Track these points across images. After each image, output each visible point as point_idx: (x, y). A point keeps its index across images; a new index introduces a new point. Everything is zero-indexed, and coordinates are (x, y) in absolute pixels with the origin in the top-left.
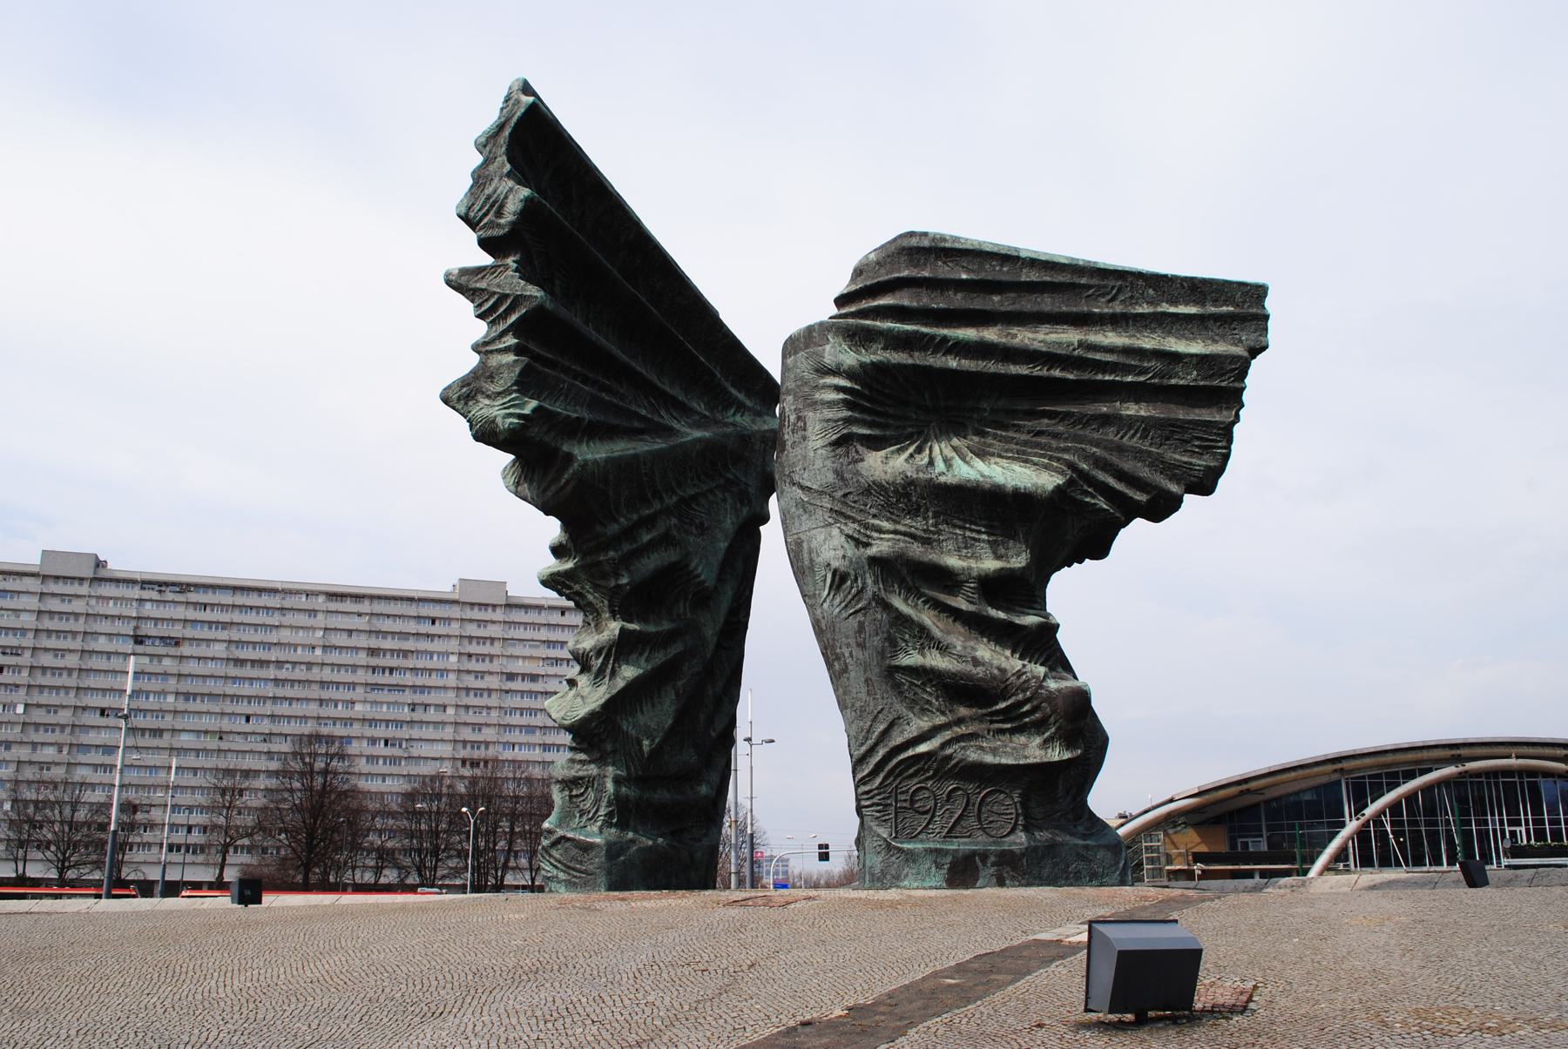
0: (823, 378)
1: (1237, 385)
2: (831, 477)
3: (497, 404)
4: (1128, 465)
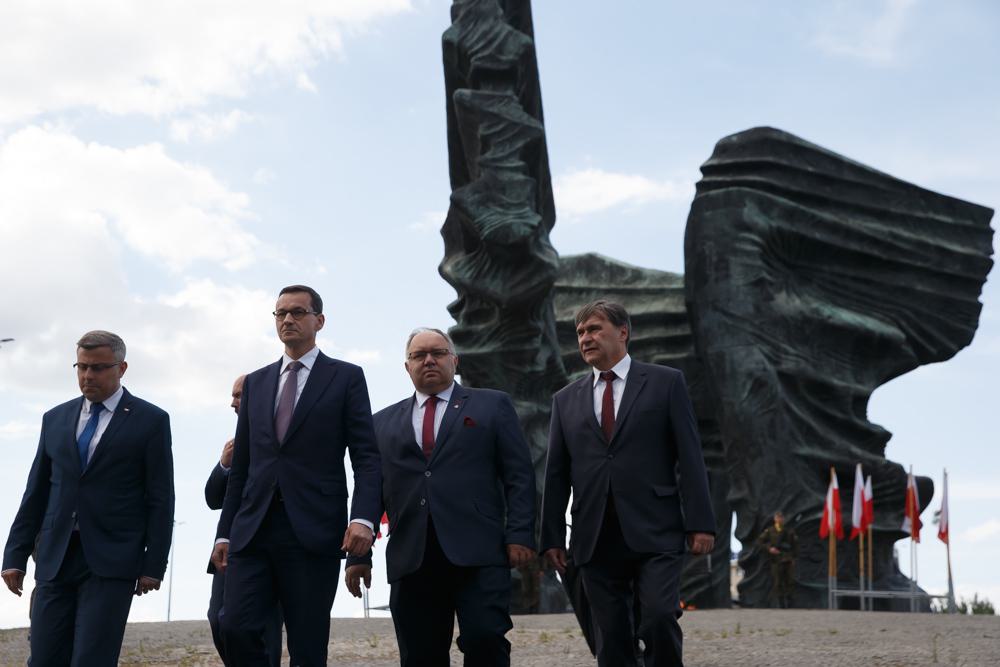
2: (751, 309)
4: (928, 328)
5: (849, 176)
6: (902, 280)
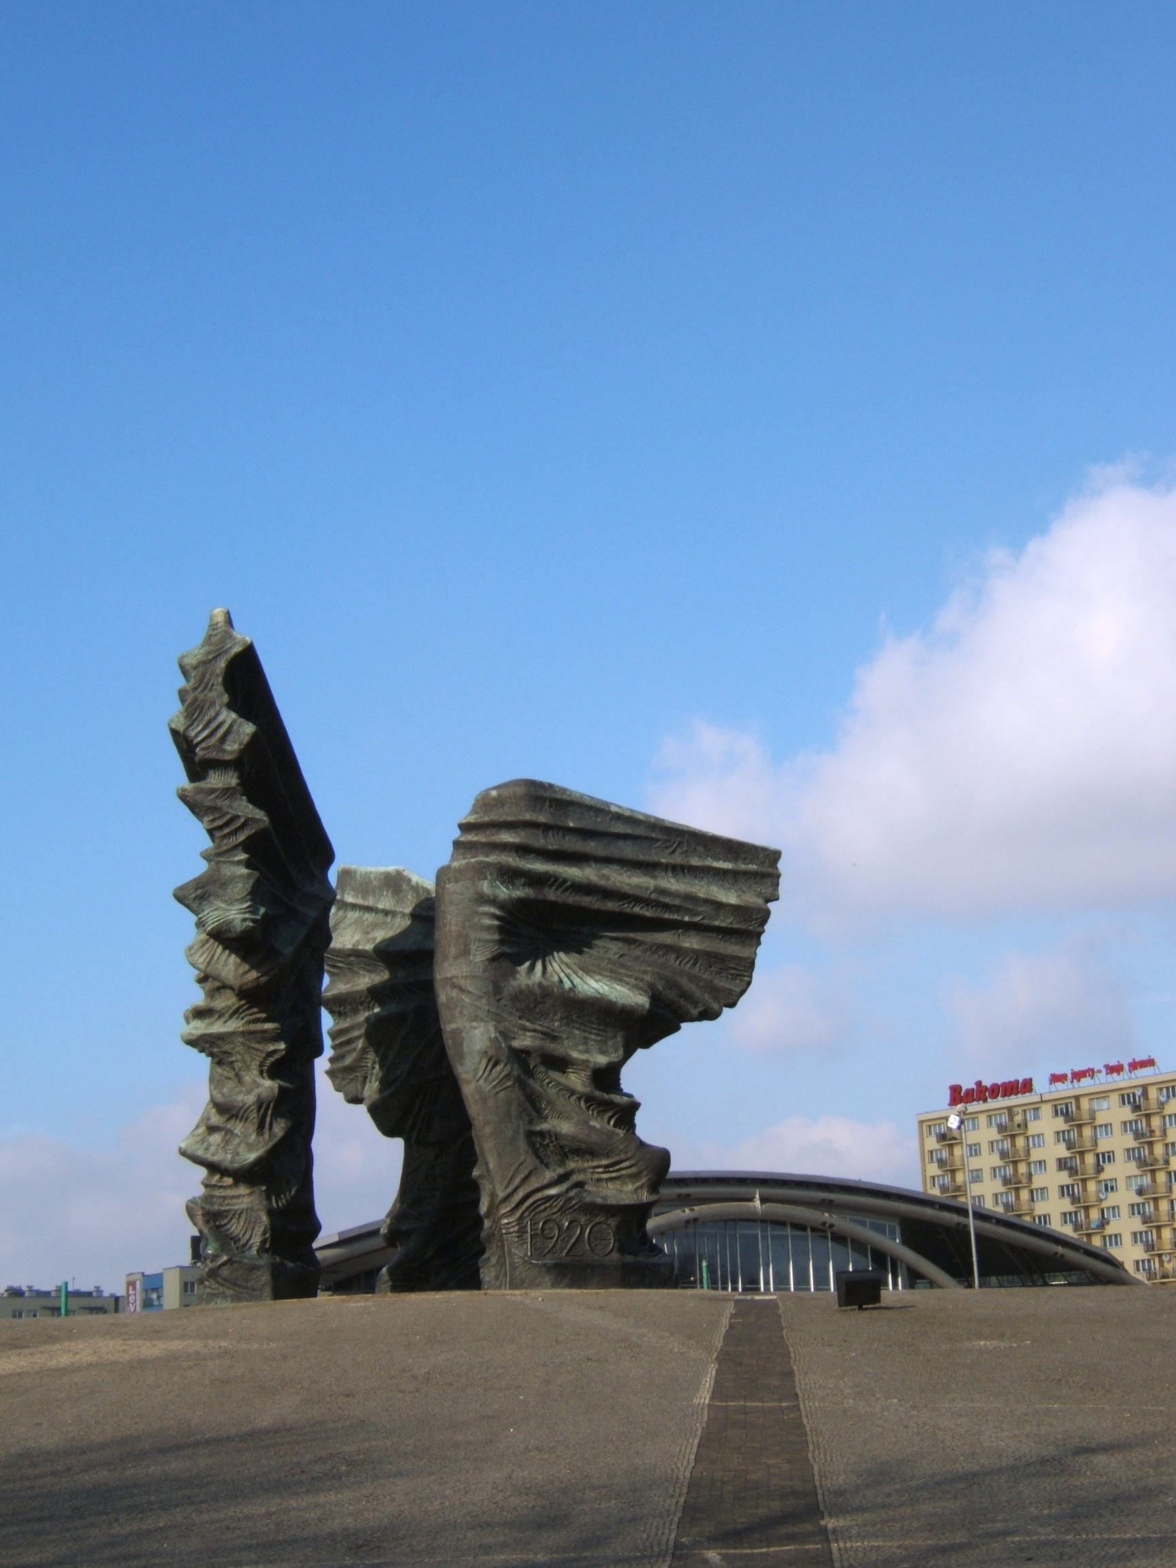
0: (481, 906)
1: (759, 929)
3: (232, 908)
5: (619, 828)
6: (666, 938)
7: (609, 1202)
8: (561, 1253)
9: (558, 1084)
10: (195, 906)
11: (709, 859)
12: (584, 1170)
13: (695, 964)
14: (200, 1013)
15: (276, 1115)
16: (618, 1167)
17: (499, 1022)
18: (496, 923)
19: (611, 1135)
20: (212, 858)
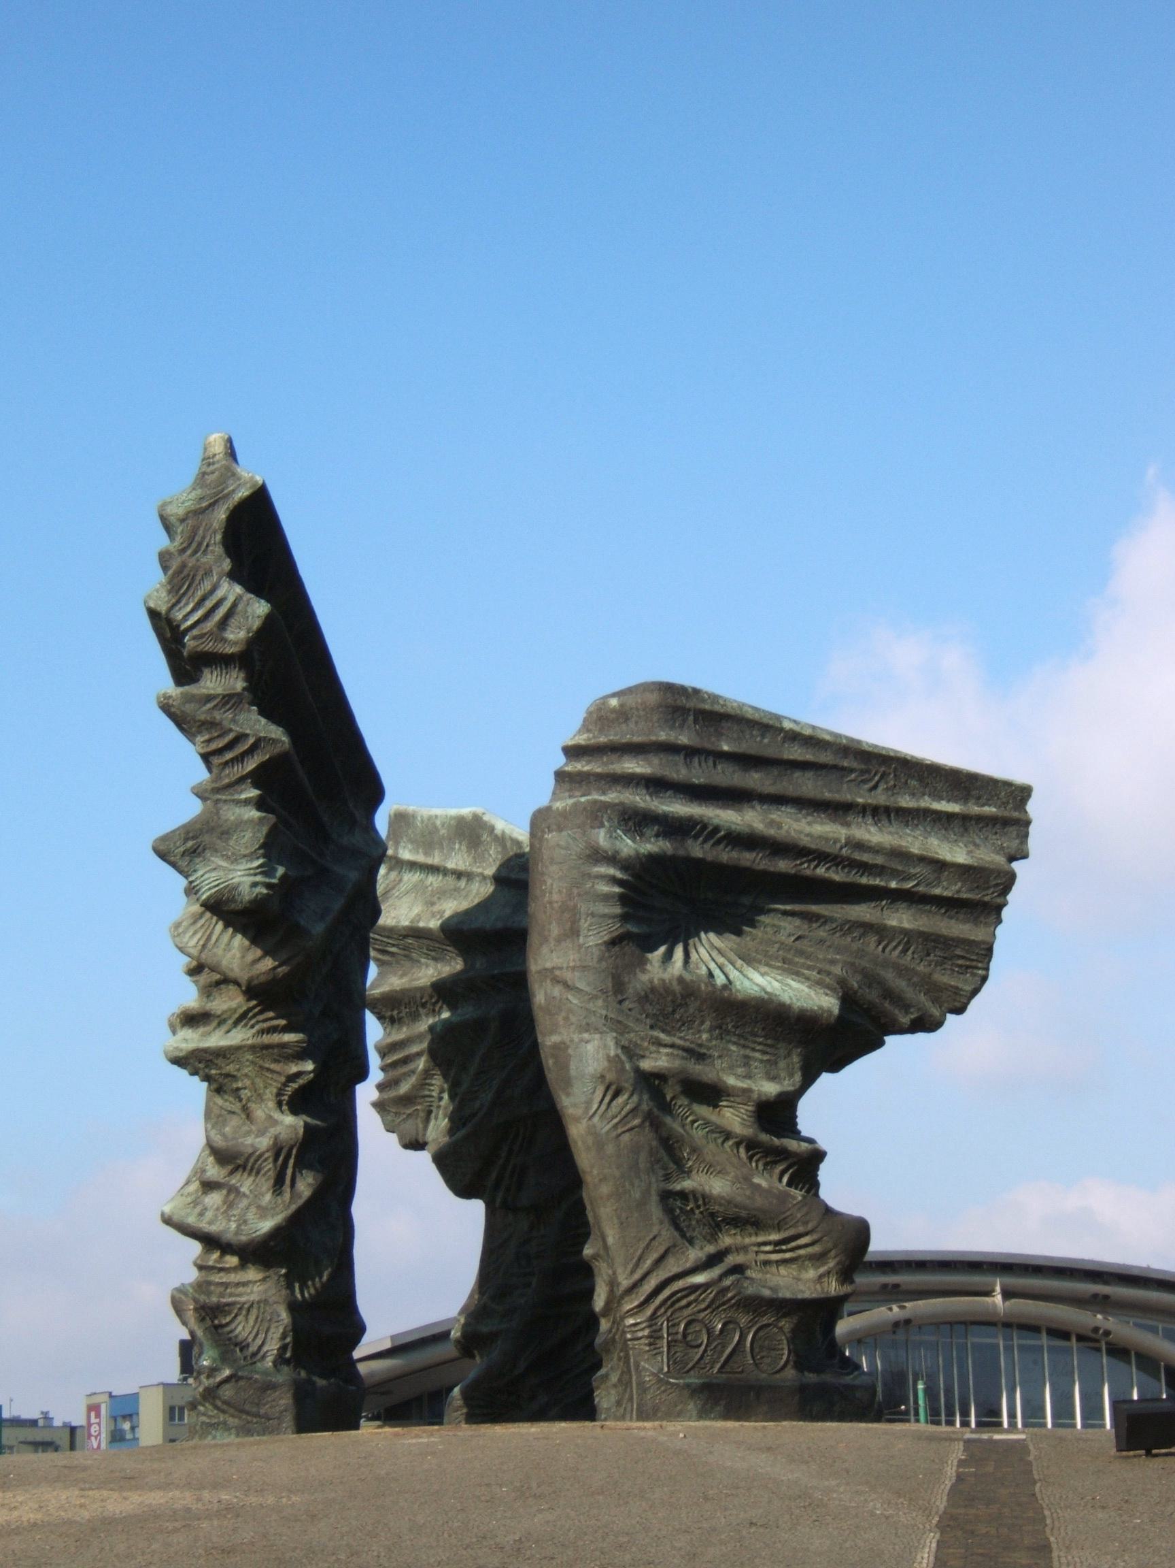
0: (595, 865)
1: (999, 900)
5: (795, 753)
6: (862, 912)
7: (781, 1295)
8: (711, 1368)
9: (707, 1123)
10: (183, 863)
11: (926, 798)
12: (744, 1249)
13: (905, 951)
14: (191, 1019)
15: (301, 1164)
16: (793, 1244)
17: (622, 1034)
18: (617, 890)
19: (783, 1198)
20: (207, 795)
